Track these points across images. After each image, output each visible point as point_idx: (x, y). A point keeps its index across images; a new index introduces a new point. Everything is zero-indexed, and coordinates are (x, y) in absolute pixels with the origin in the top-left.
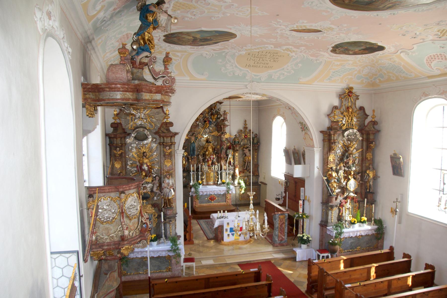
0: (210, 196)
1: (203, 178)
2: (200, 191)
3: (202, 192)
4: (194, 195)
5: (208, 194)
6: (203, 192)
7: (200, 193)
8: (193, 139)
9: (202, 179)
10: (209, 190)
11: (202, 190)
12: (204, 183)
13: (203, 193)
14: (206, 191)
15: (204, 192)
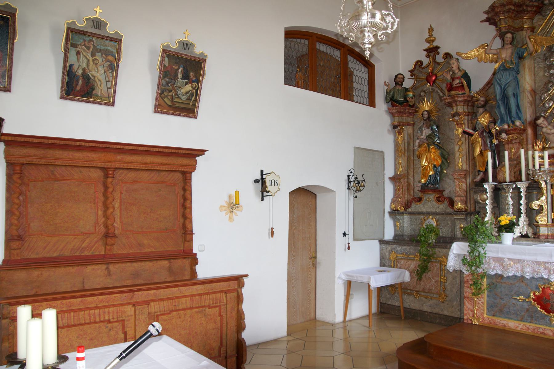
0: (537, 288)
1: (535, 205)
2: (490, 254)
3: (499, 260)
4: (466, 271)
5: (528, 276)
6: (502, 264)
7: (493, 264)
8: (503, 56)
9: (531, 214)
10: (533, 258)
11: (500, 255)
12: (543, 231)
13: (505, 268)
14: (519, 261)
15: (506, 262)
